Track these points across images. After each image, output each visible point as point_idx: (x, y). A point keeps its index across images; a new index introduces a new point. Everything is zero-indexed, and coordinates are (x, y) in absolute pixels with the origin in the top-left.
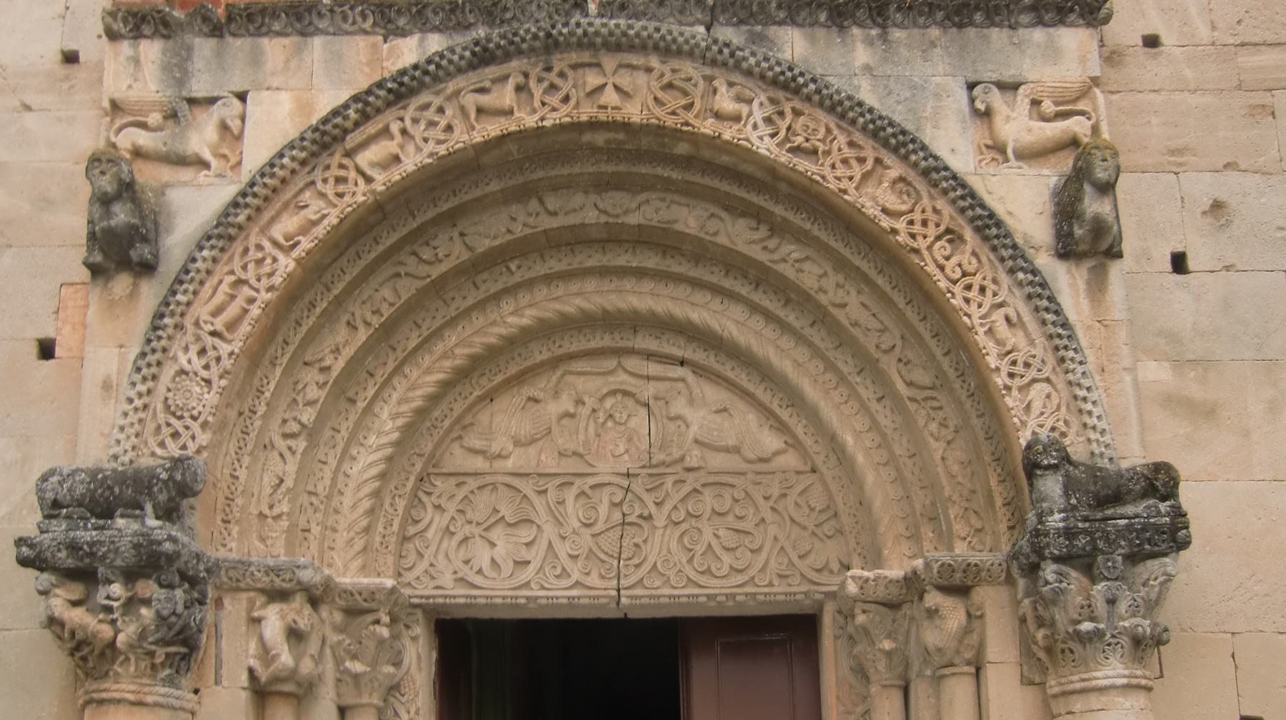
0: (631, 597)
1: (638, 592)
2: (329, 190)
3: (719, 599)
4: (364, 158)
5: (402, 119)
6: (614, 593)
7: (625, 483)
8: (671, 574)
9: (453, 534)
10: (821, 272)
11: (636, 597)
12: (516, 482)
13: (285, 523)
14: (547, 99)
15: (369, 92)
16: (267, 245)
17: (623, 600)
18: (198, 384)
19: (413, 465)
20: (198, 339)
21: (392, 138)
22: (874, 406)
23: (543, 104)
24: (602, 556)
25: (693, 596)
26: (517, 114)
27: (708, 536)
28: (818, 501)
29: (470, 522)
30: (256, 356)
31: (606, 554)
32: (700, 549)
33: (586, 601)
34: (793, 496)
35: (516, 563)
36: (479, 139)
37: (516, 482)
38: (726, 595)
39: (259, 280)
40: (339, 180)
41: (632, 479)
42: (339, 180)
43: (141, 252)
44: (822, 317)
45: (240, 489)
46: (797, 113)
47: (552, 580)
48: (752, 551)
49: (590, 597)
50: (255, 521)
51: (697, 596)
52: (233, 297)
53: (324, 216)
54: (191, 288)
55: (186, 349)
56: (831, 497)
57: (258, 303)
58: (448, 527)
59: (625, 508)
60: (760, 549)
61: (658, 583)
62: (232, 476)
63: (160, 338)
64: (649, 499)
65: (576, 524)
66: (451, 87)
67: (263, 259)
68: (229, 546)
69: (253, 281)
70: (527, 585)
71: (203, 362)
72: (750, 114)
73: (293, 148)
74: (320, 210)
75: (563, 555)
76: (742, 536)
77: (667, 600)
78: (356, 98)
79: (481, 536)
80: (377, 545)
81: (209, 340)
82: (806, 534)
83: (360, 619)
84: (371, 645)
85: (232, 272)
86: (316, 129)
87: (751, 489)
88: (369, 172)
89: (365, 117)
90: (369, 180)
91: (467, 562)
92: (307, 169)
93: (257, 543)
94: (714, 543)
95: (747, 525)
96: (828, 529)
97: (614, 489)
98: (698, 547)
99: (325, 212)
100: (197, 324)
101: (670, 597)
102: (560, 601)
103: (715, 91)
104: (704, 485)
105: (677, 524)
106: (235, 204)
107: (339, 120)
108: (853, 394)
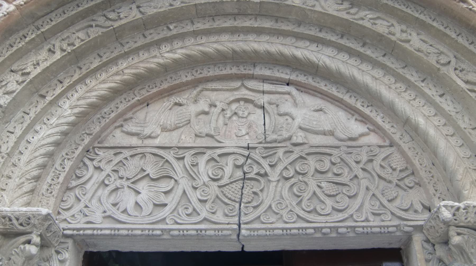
0: (250, 230)
1: (256, 225)
3: (324, 231)
6: (236, 227)
7: (246, 153)
8: (284, 213)
9: (107, 185)
11: (254, 230)
12: (161, 152)
17: (243, 232)
19: (83, 140)
24: (226, 200)
25: (302, 228)
29: (121, 178)
31: (230, 199)
32: (306, 195)
33: (212, 233)
35: (155, 205)
37: (161, 152)
38: (330, 228)
41: (250, 150)
47: (184, 217)
48: (350, 197)
49: (215, 230)
51: (306, 228)
58: (103, 182)
59: (246, 169)
60: (355, 196)
64: (265, 164)
65: (206, 179)
70: (163, 220)
75: (194, 200)
76: (340, 187)
77: (280, 232)
79: (129, 187)
80: (44, 191)
87: (344, 156)
91: (115, 205)
94: (318, 191)
97: (238, 157)
98: (305, 194)
101: (283, 229)
102: (190, 232)
104: (308, 154)
105: (287, 179)
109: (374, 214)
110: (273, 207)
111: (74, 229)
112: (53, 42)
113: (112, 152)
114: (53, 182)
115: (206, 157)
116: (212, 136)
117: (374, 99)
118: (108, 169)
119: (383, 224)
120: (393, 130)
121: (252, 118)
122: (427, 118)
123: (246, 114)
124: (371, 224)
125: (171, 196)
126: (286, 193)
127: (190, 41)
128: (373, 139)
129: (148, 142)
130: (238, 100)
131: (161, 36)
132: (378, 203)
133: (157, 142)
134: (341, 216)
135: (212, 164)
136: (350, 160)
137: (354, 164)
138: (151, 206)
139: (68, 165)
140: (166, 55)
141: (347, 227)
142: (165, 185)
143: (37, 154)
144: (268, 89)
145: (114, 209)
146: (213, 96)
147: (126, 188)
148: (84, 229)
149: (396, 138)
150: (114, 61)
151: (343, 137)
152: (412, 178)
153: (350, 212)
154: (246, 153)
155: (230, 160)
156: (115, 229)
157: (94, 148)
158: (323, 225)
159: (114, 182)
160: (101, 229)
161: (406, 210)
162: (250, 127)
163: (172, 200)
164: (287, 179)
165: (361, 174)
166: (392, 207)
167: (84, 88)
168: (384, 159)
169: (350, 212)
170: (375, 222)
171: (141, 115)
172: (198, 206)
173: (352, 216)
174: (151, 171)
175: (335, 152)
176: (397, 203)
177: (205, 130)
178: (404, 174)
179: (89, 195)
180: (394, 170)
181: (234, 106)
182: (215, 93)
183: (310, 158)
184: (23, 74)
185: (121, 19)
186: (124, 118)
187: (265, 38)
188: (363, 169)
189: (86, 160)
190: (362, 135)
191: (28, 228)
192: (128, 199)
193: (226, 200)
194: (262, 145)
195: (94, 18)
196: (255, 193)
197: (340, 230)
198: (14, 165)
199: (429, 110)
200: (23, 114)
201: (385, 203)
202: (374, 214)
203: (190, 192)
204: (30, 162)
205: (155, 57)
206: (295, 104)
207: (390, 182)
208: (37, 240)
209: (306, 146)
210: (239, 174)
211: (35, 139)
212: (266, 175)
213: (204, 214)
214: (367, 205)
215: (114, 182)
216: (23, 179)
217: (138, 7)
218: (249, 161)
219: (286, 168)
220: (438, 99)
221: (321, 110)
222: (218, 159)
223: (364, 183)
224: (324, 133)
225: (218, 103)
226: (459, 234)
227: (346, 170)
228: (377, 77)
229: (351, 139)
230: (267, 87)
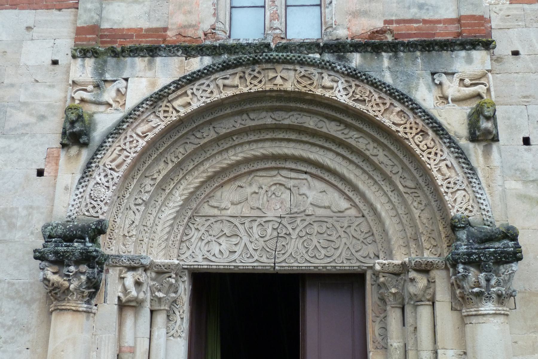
1: (283, 264)
2: (161, 115)
3: (319, 268)
4: (176, 104)
5: (192, 89)
6: (273, 265)
8: (298, 258)
10: (367, 142)
11: (282, 267)
13: (134, 239)
14: (253, 82)
15: (179, 80)
16: (134, 135)
17: (277, 268)
18: (104, 188)
20: (104, 171)
21: (188, 96)
22: (390, 193)
23: (251, 84)
25: (308, 266)
26: (240, 87)
27: (315, 242)
28: (365, 228)
30: (127, 176)
32: (311, 248)
33: (260, 268)
34: (354, 226)
36: (224, 97)
38: (323, 267)
39: (131, 149)
40: (165, 111)
42: (165, 111)
43: (84, 139)
44: (366, 159)
45: (117, 226)
46: (357, 86)
48: (335, 249)
49: (262, 266)
50: (122, 238)
51: (310, 267)
52: (120, 155)
53: (159, 125)
54: (103, 153)
55: (99, 174)
56: (370, 228)
57: (129, 158)
61: (292, 261)
62: (114, 221)
63: (90, 171)
66: (213, 77)
67: (133, 141)
68: (111, 249)
69: (128, 150)
71: (106, 180)
72: (337, 86)
73: (147, 100)
74: (157, 123)
76: (330, 243)
77: (296, 268)
78: (174, 82)
81: (109, 172)
82: (359, 242)
83: (163, 276)
84: (167, 286)
85: (120, 146)
86: (157, 94)
88: (178, 109)
89: (177, 89)
90: (178, 112)
92: (153, 107)
93: (122, 246)
94: (318, 245)
95: (333, 238)
96: (369, 240)
98: (311, 247)
99: (159, 123)
100: (104, 165)
101: (297, 267)
103: (323, 78)
106: (123, 122)
107: (166, 90)
108: (381, 188)
109: (347, 259)
110: (293, 254)
111: (188, 265)
112: (166, 156)
113: (204, 219)
114: (174, 240)
115: (257, 223)
116: (260, 209)
117: (355, 189)
118: (203, 230)
119: (351, 265)
120: (364, 208)
121: (283, 196)
122: (382, 204)
123: (280, 194)
124: (344, 265)
125: (239, 245)
126: (300, 246)
127: (246, 147)
128: (353, 212)
129: (224, 212)
130: (275, 184)
131: (228, 145)
132: (350, 253)
133: (229, 212)
134: (329, 260)
135: (260, 227)
136: (338, 226)
137: (340, 228)
138: (228, 253)
139: (181, 229)
140: (232, 158)
141: (332, 266)
142: (235, 240)
143: (165, 226)
144: (294, 177)
145: (208, 254)
146: (261, 180)
147: (214, 242)
148: (193, 265)
149: (365, 213)
150: (202, 163)
151: (335, 210)
152: (371, 238)
153: (334, 258)
154: (279, 220)
155: (270, 225)
156: (210, 265)
157: (193, 216)
158: (318, 265)
159: (207, 238)
160: (202, 265)
161: (365, 257)
162: (282, 203)
163: (239, 249)
164: (301, 237)
165: (343, 235)
166: (357, 255)
167: (186, 181)
168: (357, 226)
169: (334, 258)
170: (347, 264)
171: (218, 194)
172: (253, 253)
173: (335, 260)
174: (226, 231)
175: (330, 220)
176: (360, 253)
177: (256, 205)
178: (367, 235)
179: (194, 246)
180: (362, 232)
181: (273, 188)
182: (262, 178)
183: (315, 224)
184: (152, 179)
185: (204, 138)
186: (209, 196)
187: (292, 145)
188: (344, 231)
189: (190, 224)
190: (347, 209)
191: (169, 270)
192: (215, 248)
193: (268, 250)
194: (289, 216)
195: (188, 137)
196: (283, 245)
197: (328, 268)
198: (154, 232)
199: (384, 200)
200: (154, 202)
201: (353, 251)
202: (347, 259)
203: (248, 244)
204: (162, 230)
205: (225, 159)
206: (309, 188)
207: (359, 240)
208: (174, 276)
209: (313, 217)
210: (275, 234)
211: (163, 216)
212: (290, 234)
213: (256, 258)
214: (344, 254)
215: (207, 238)
216: (161, 241)
217: (214, 128)
218: (281, 225)
219: (301, 230)
220: (390, 193)
221: (324, 191)
222: (263, 224)
223: (344, 240)
224: (325, 207)
225: (263, 187)
226: (383, 276)
227: (335, 232)
228: (358, 175)
229: (340, 212)
230: (293, 175)
